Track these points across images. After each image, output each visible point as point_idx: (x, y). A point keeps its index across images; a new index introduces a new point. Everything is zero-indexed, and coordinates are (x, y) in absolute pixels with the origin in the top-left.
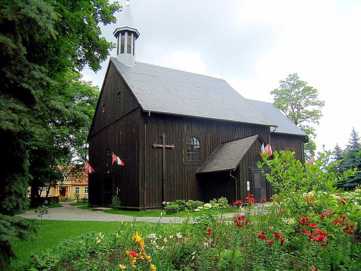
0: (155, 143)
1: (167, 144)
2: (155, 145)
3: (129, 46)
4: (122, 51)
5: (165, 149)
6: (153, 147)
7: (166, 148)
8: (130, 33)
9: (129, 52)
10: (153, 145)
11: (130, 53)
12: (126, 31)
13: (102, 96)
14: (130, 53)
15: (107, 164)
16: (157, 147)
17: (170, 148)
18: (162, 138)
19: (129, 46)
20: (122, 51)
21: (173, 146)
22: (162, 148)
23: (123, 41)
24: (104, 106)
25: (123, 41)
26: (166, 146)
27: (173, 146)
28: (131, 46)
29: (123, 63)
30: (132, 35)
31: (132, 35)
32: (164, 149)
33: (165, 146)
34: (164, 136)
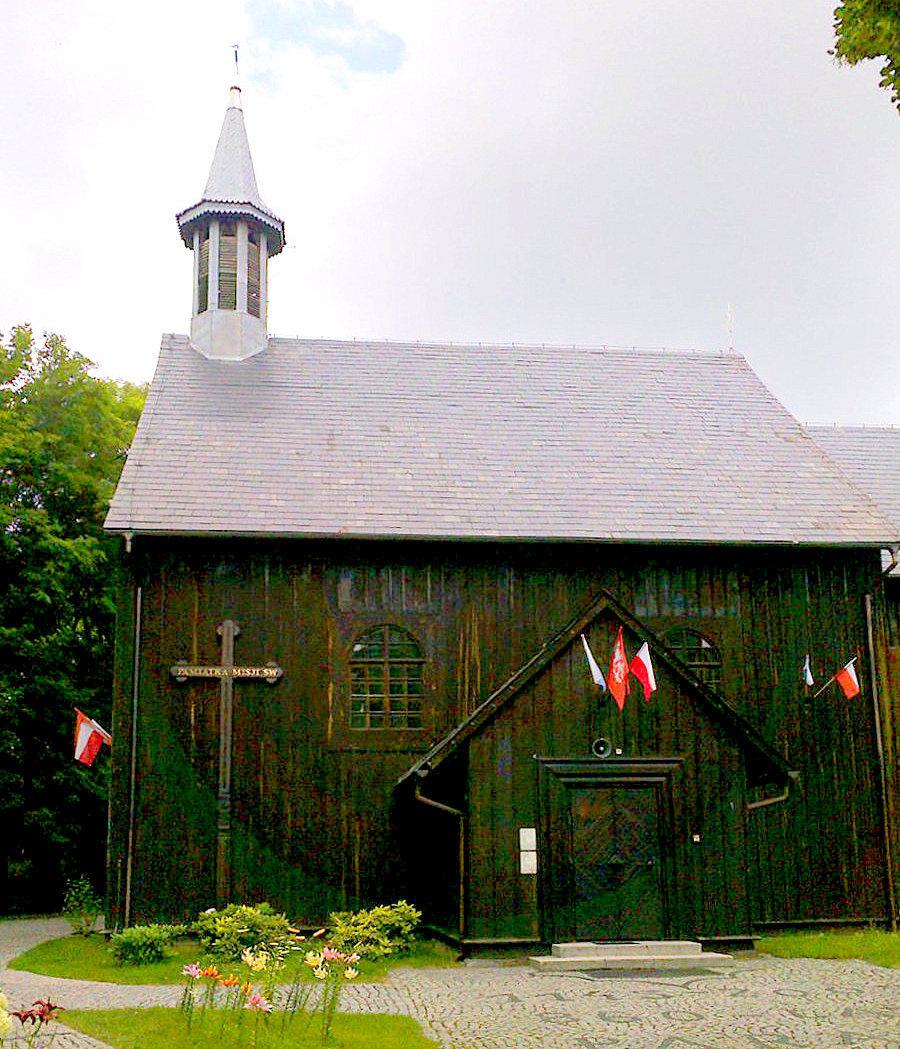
2: (183, 671)
3: (228, 281)
6: (172, 678)
8: (228, 222)
12: (209, 217)
16: (193, 681)
18: (219, 639)
19: (228, 281)
20: (203, 307)
21: (273, 672)
22: (215, 681)
26: (237, 672)
27: (273, 672)
28: (235, 275)
30: (242, 233)
31: (242, 233)
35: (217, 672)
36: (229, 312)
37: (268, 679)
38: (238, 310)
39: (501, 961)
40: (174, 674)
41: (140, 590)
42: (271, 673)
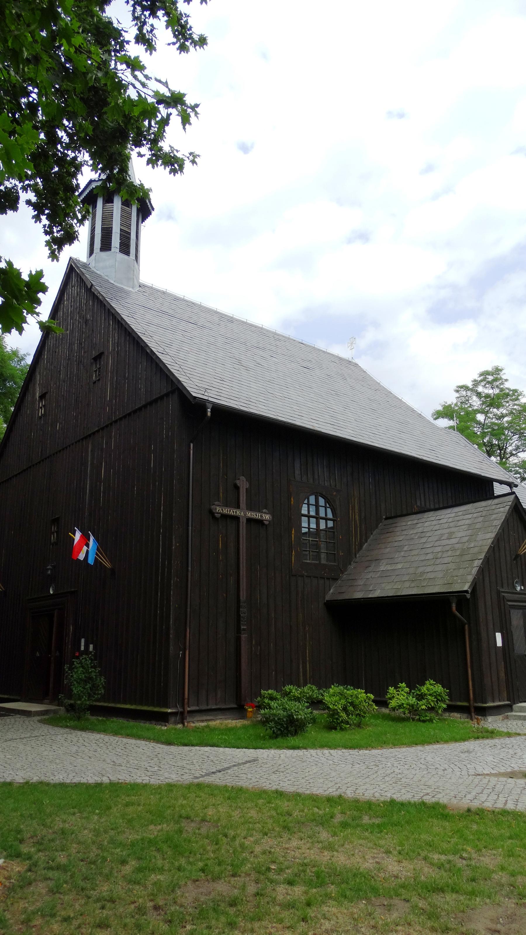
0: (216, 503)
1: (250, 508)
2: (219, 510)
4: (106, 246)
5: (245, 521)
6: (211, 513)
7: (250, 520)
9: (125, 248)
10: (213, 507)
11: (127, 253)
13: (38, 370)
14: (127, 253)
15: (49, 567)
16: (225, 517)
17: (260, 522)
20: (106, 246)
22: (236, 519)
23: (107, 218)
24: (42, 397)
25: (107, 218)
26: (249, 514)
29: (106, 278)
32: (243, 522)
33: (245, 515)
34: (243, 483)
35: (238, 513)
36: (126, 257)
37: (265, 522)
38: (131, 257)
39: (500, 717)
40: (214, 511)
41: (192, 445)
42: (267, 517)
